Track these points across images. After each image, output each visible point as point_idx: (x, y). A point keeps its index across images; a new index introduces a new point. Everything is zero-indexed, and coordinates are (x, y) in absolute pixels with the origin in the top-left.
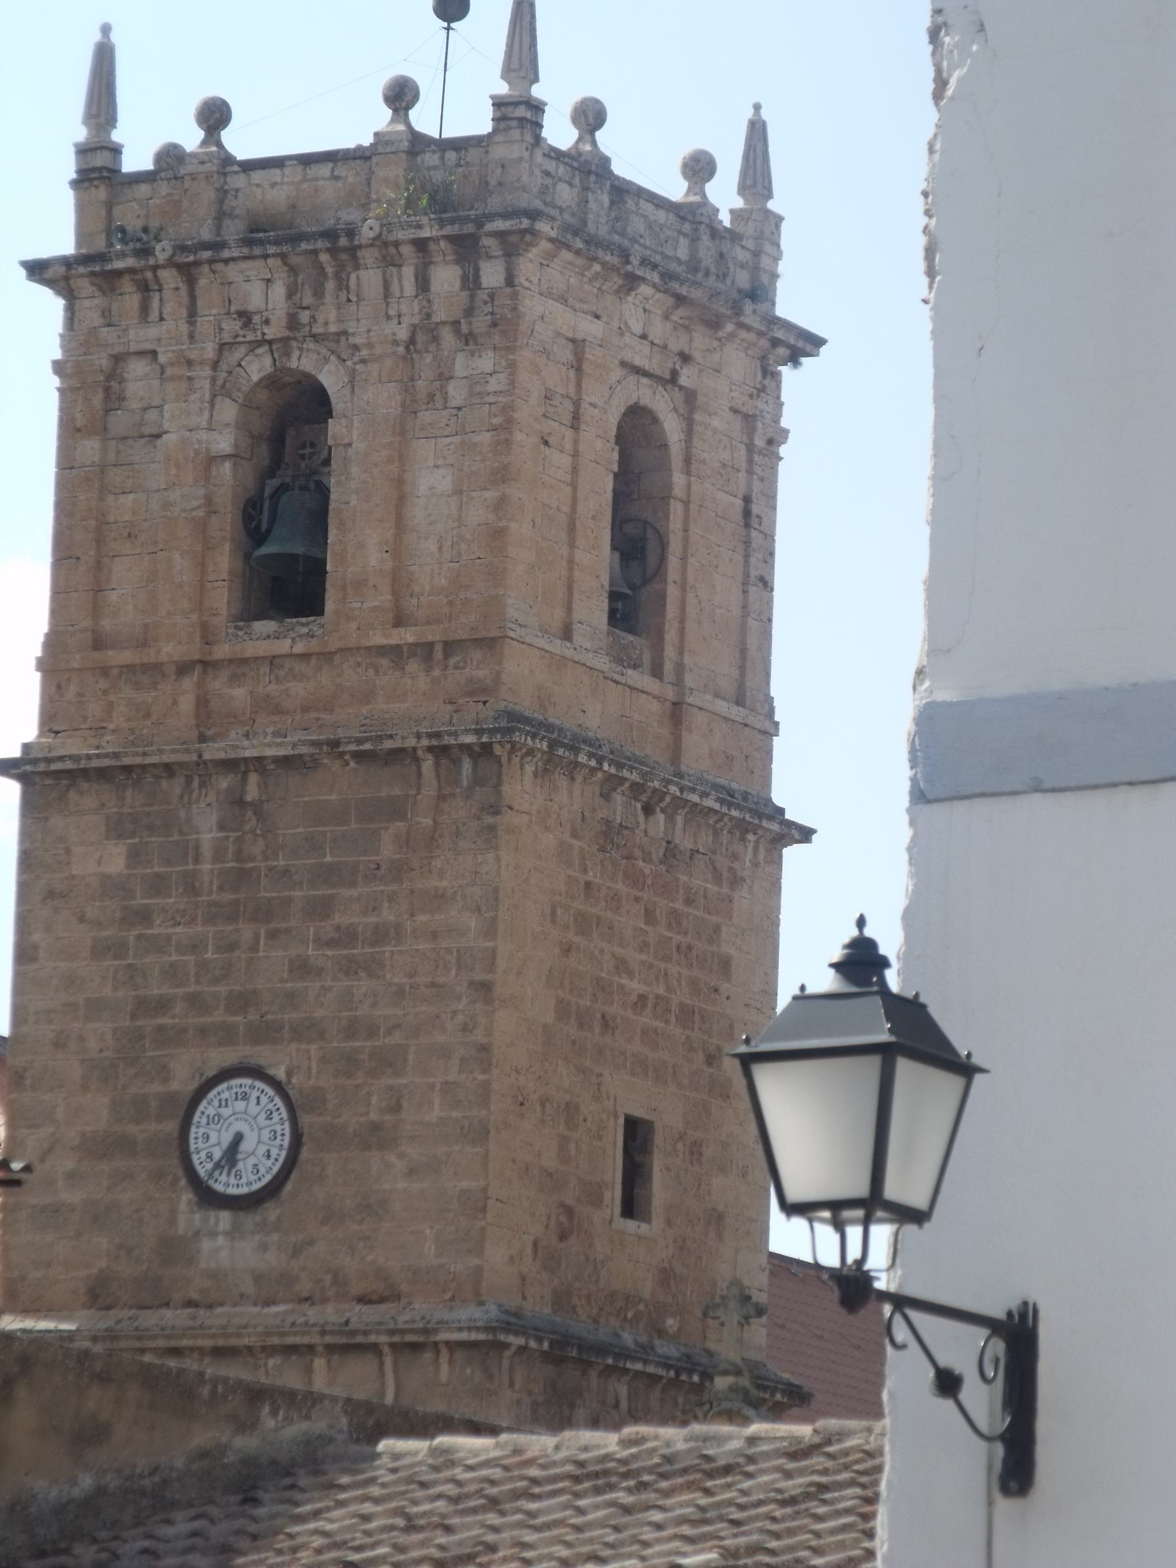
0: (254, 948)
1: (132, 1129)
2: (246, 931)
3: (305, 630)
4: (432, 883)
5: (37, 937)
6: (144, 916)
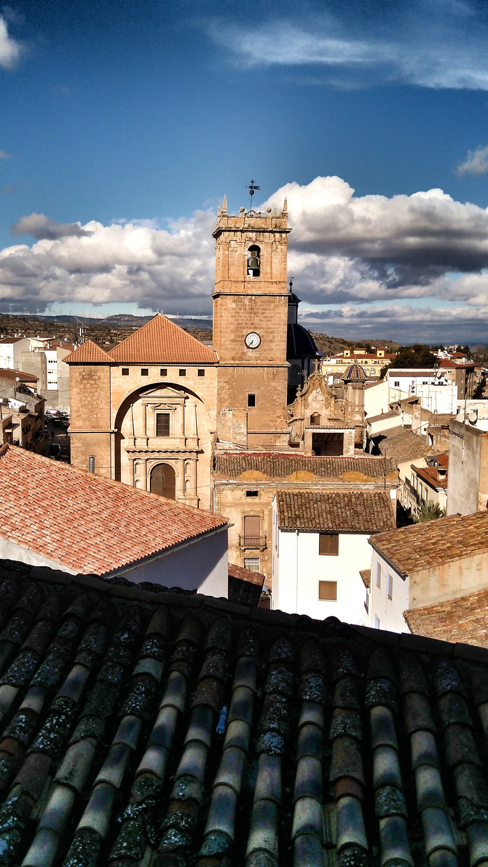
0: (254, 318)
1: (238, 339)
2: (253, 315)
5: (223, 314)
6: (239, 313)
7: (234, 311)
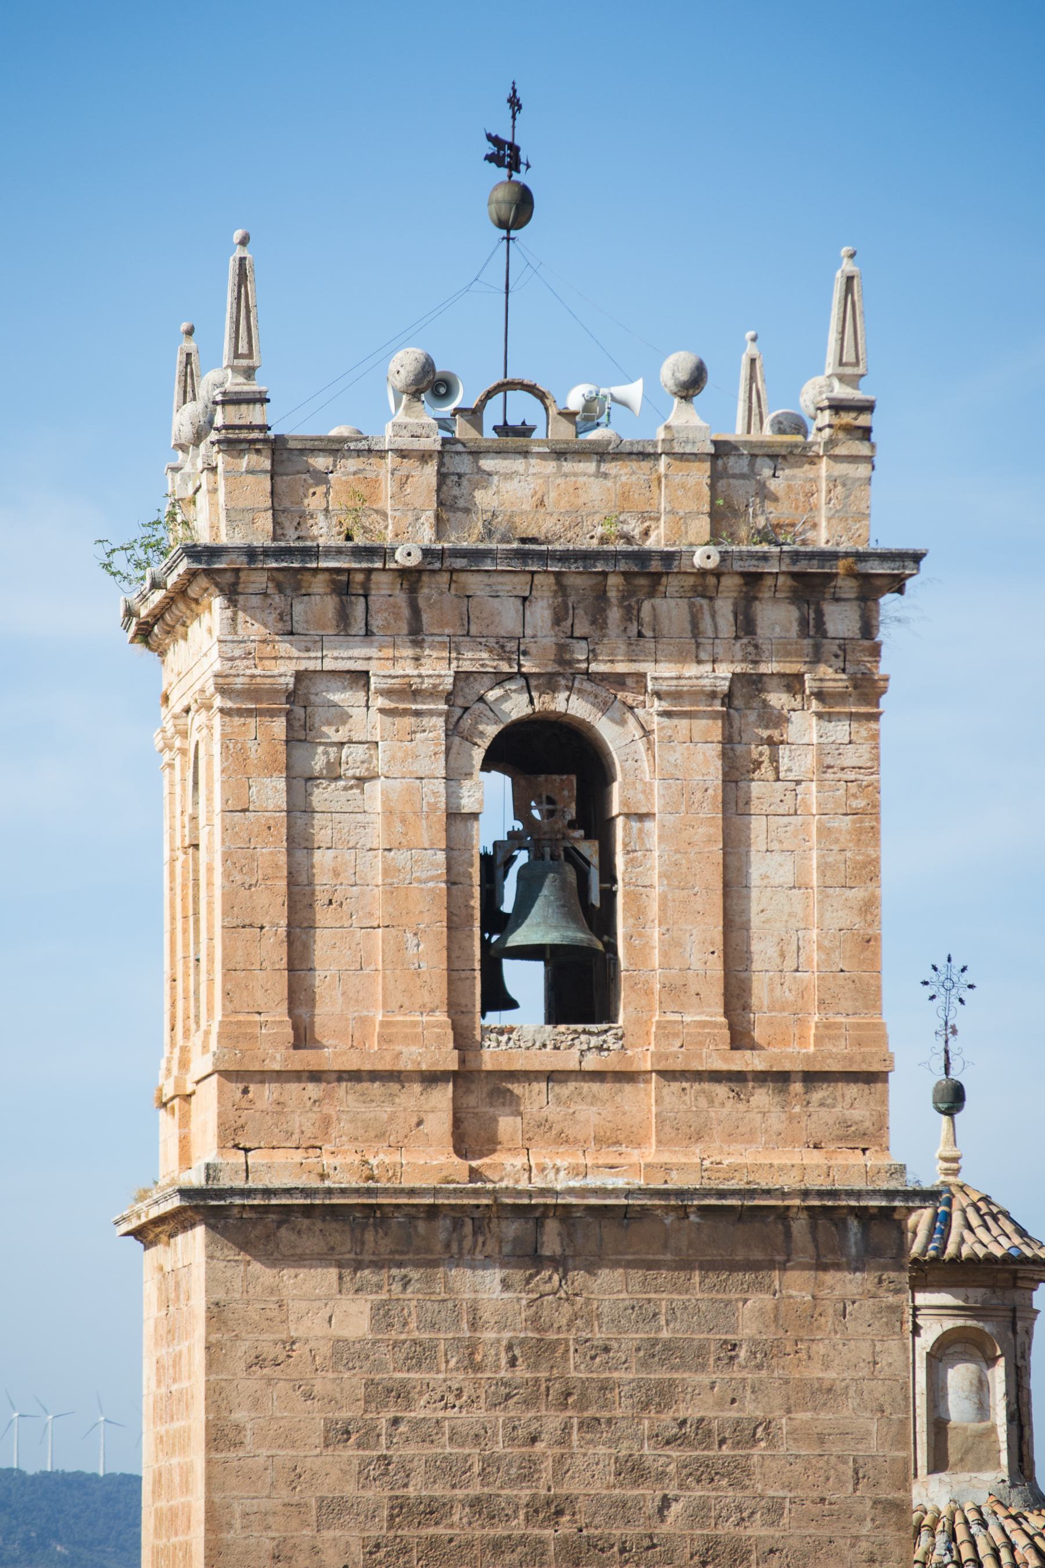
2: (553, 1421)
3: (594, 1041)
4: (815, 1372)
5: (239, 1416)
6: (402, 1394)
7: (354, 1381)
